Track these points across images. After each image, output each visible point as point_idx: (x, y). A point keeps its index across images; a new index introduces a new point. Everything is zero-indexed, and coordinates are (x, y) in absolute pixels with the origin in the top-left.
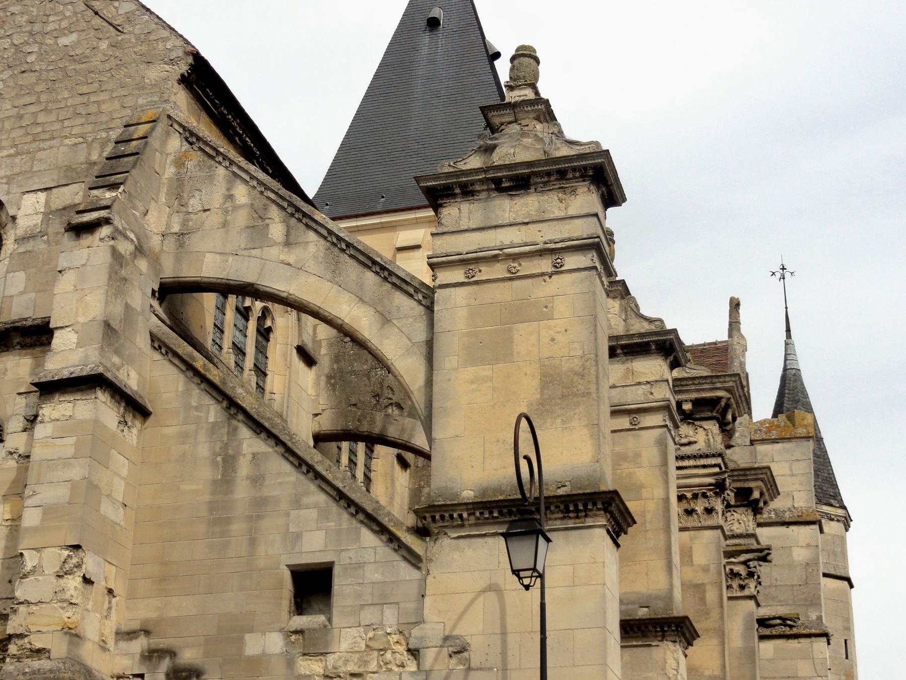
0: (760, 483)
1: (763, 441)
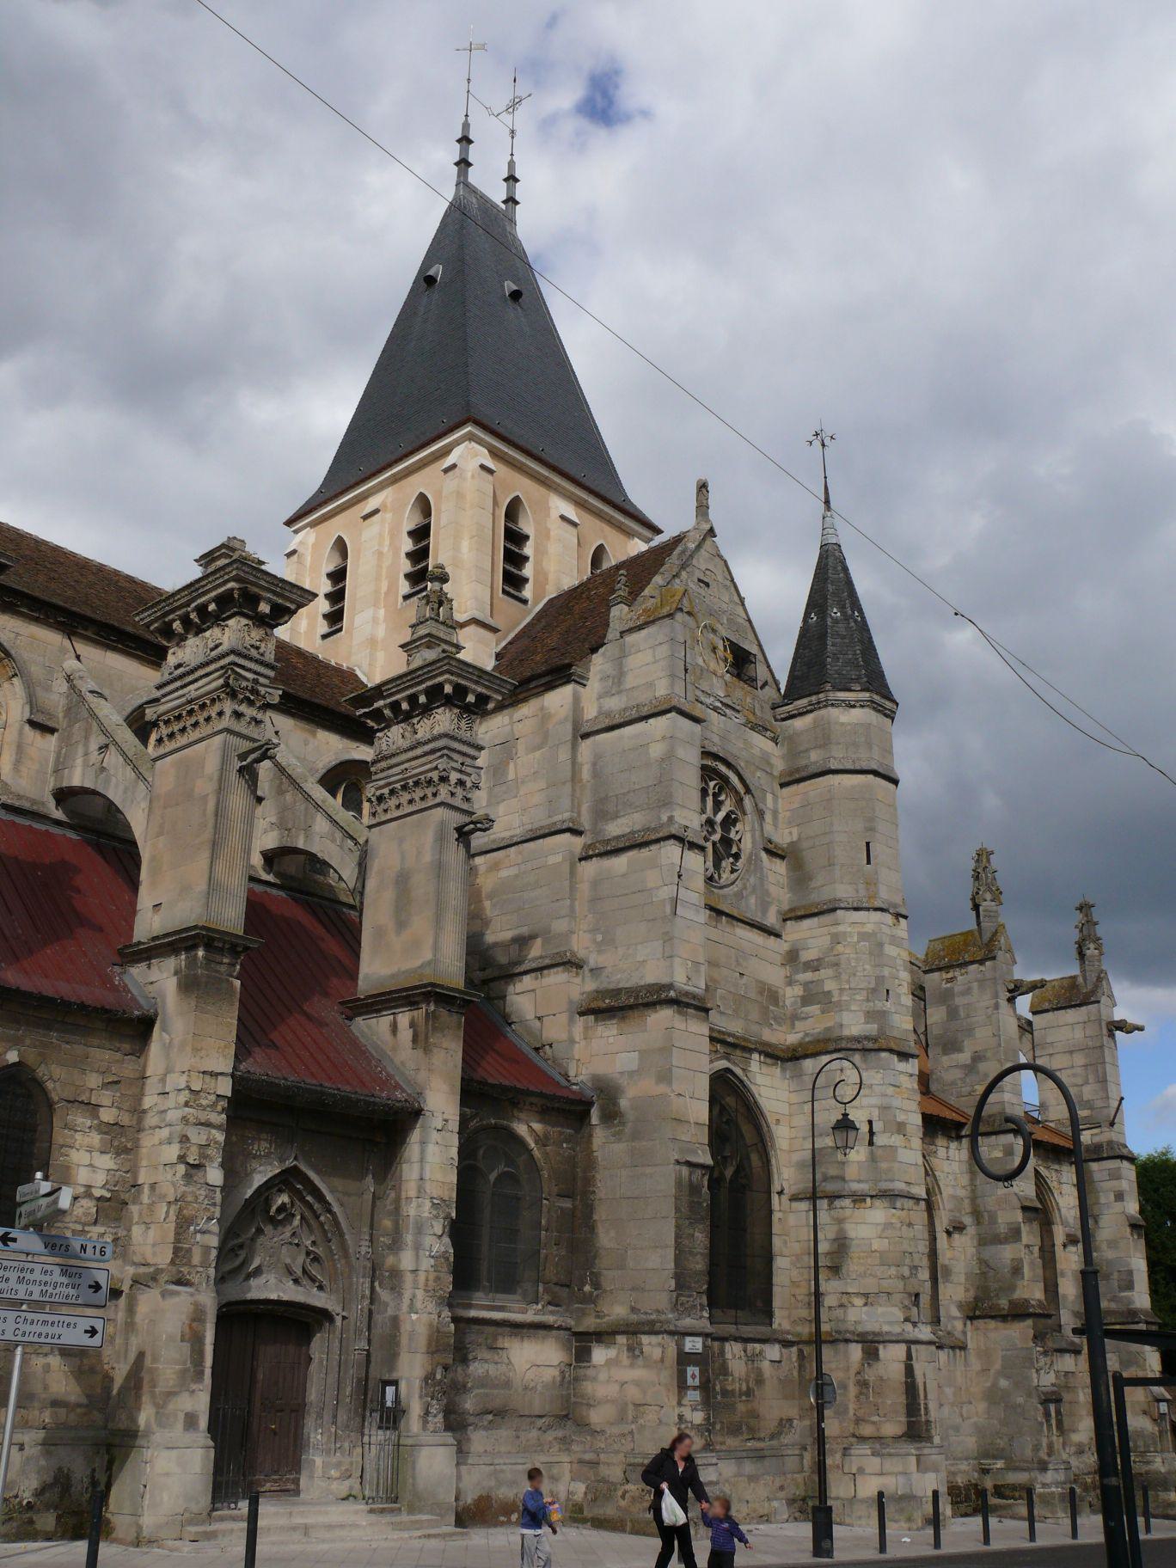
0: (447, 676)
1: (631, 630)
